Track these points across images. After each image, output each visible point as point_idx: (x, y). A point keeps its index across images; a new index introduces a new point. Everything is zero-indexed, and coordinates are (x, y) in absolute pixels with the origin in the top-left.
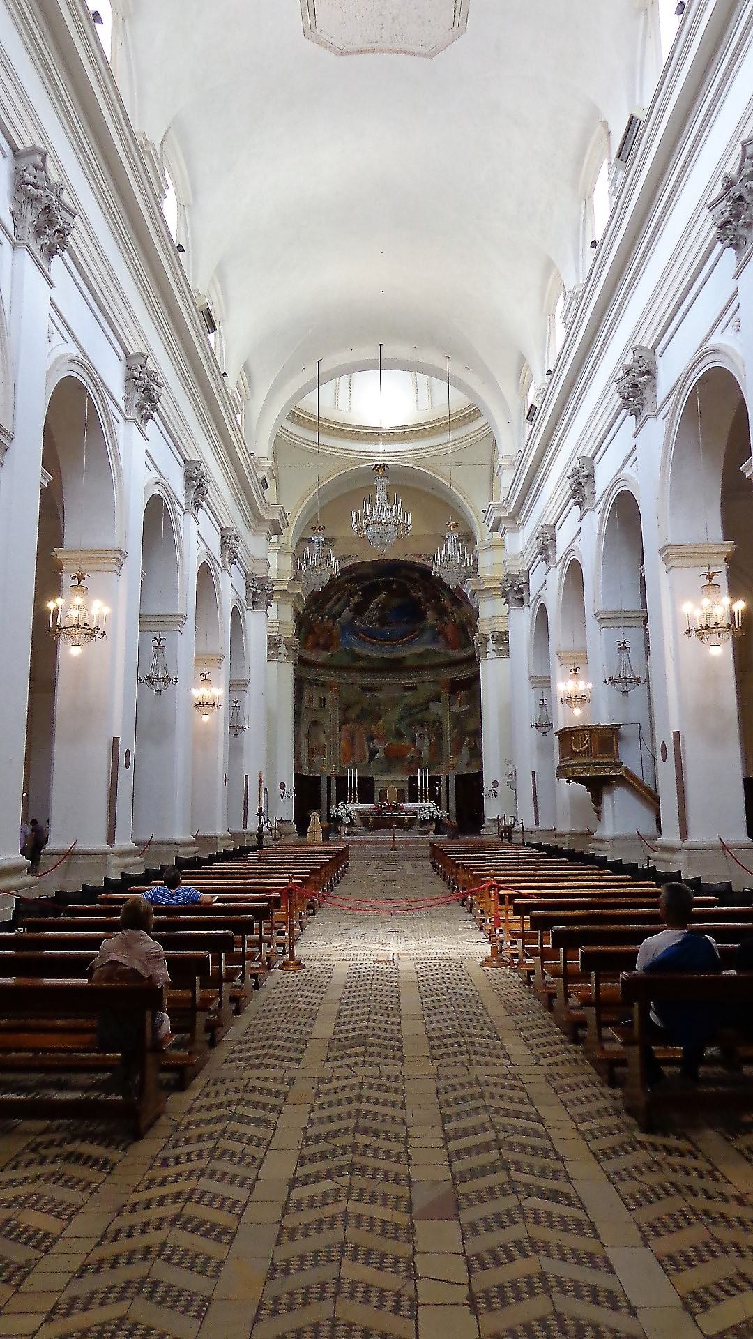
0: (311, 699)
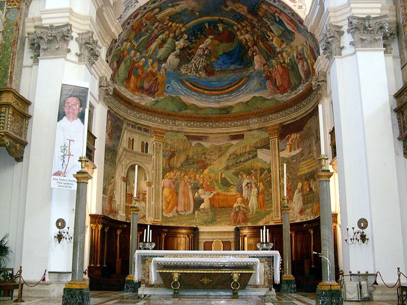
0: (131, 142)
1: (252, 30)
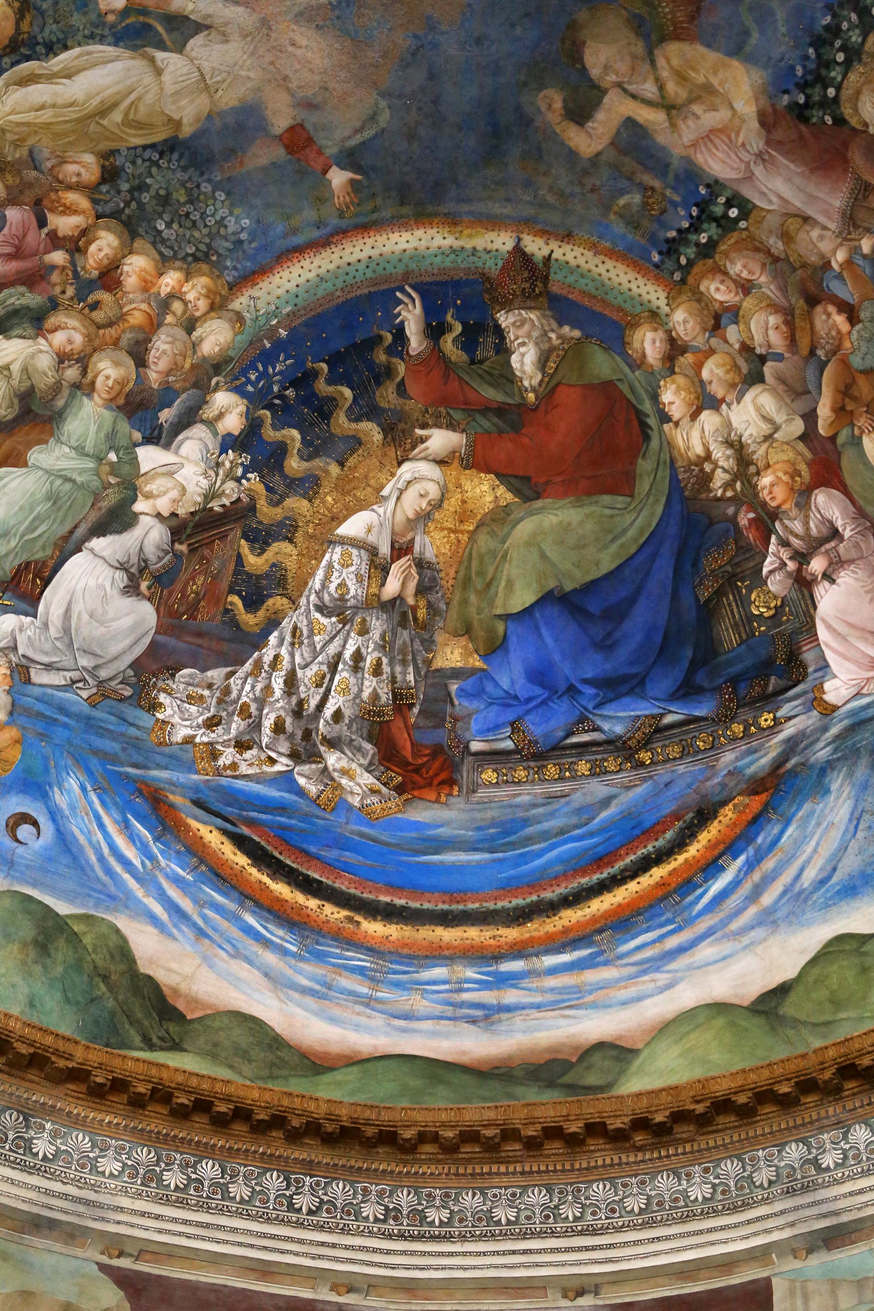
1: (792, 341)
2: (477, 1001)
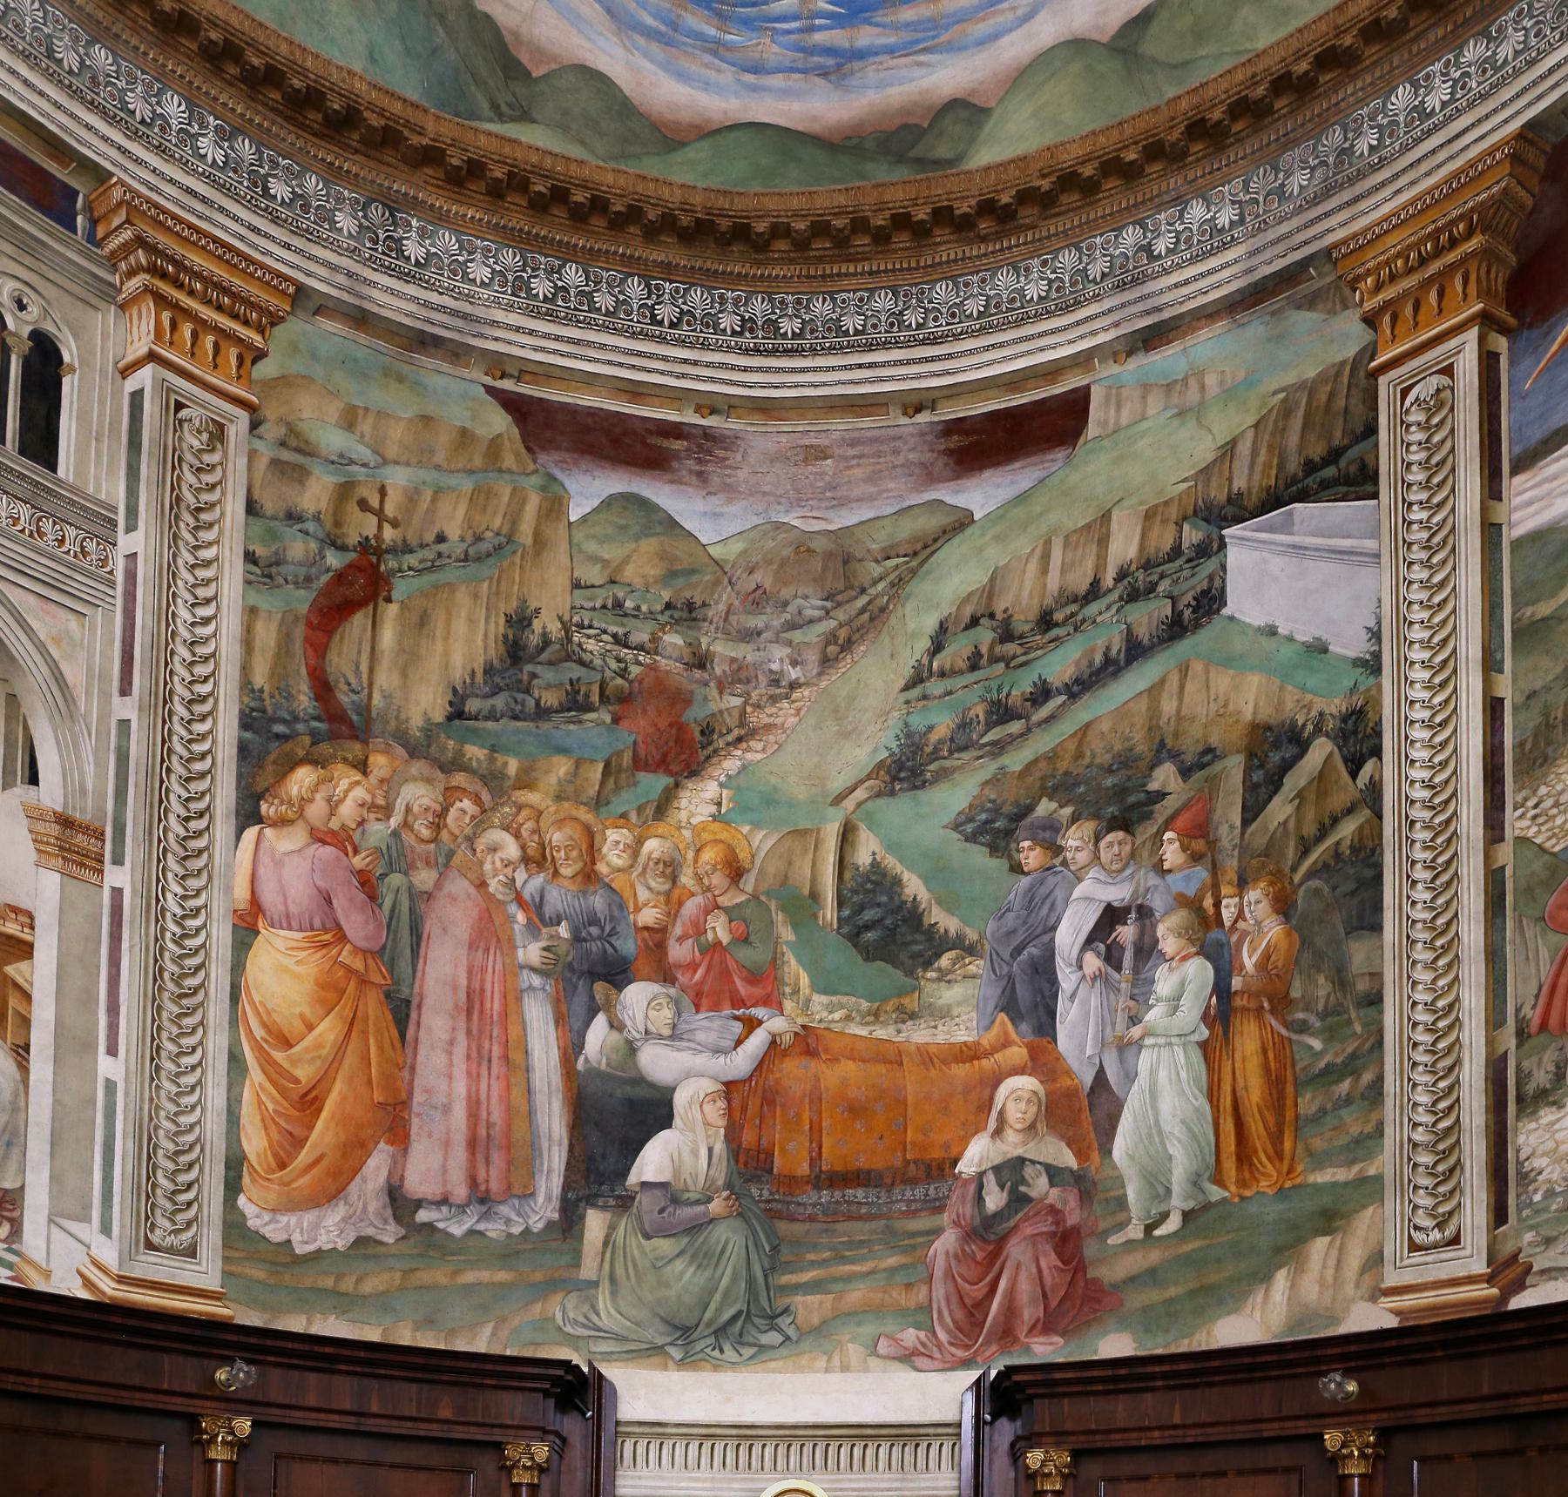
2: (828, 44)
